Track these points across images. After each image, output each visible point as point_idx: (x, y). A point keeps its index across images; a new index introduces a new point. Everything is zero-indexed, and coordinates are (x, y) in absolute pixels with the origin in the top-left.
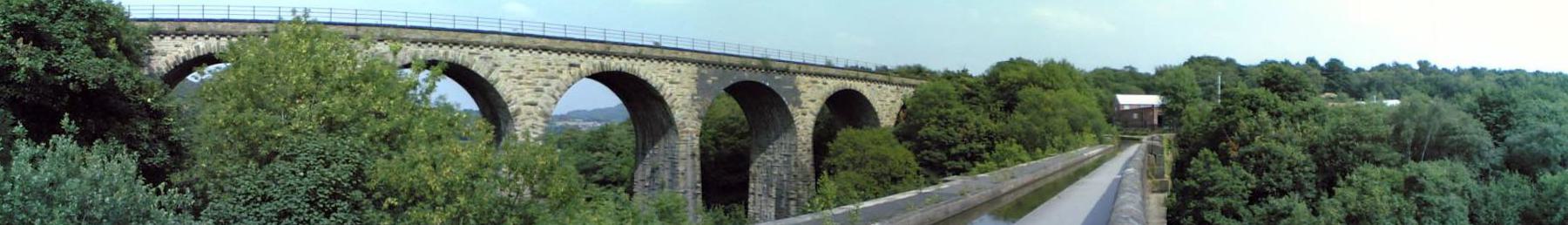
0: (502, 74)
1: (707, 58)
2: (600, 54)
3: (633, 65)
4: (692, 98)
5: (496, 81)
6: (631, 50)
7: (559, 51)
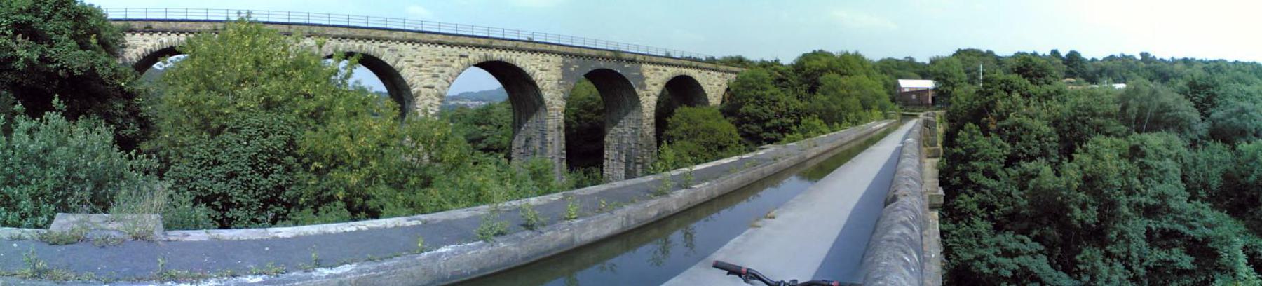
0: (406, 63)
1: (570, 50)
2: (484, 47)
3: (511, 56)
4: (559, 83)
5: (401, 69)
6: (510, 44)
7: (452, 45)
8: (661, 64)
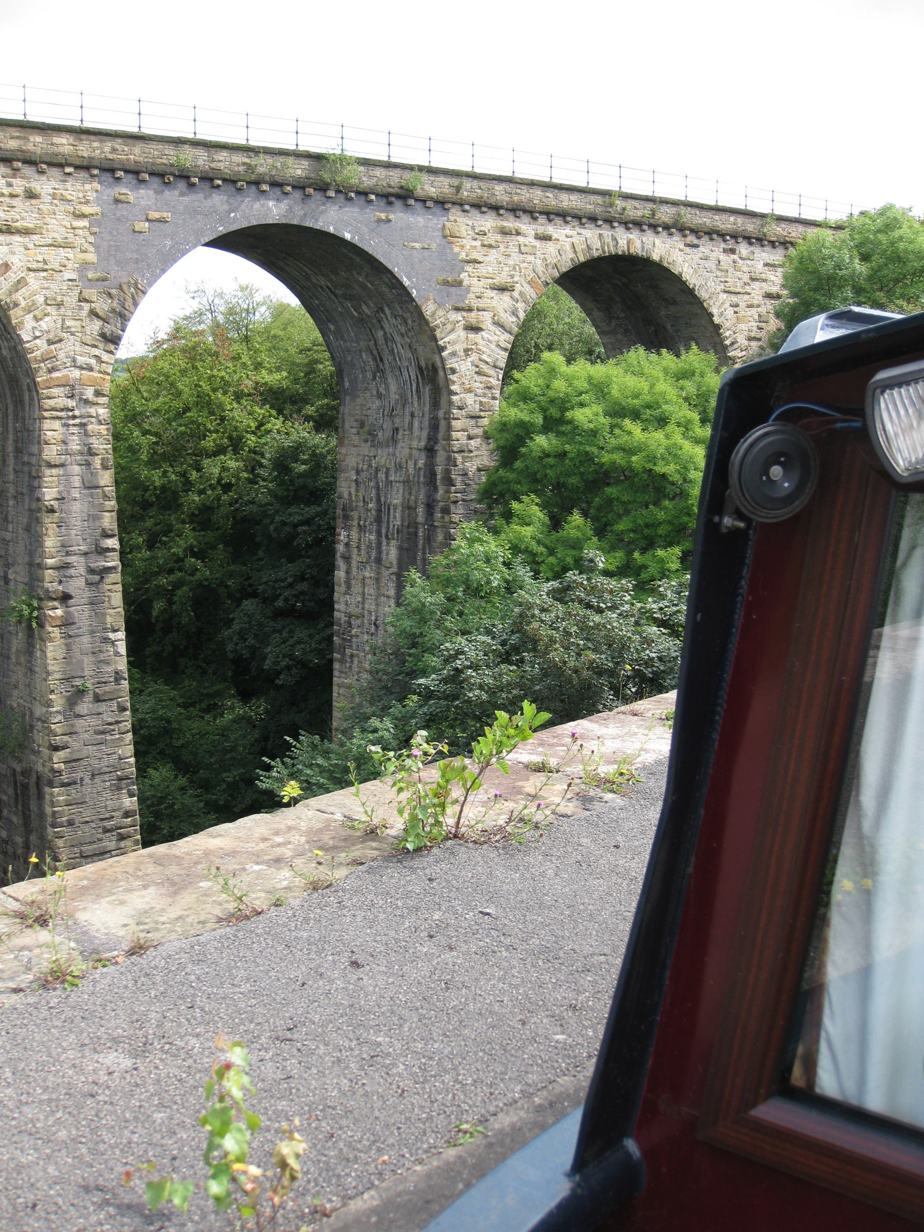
1: (135, 154)
4: (82, 276)
8: (531, 213)
